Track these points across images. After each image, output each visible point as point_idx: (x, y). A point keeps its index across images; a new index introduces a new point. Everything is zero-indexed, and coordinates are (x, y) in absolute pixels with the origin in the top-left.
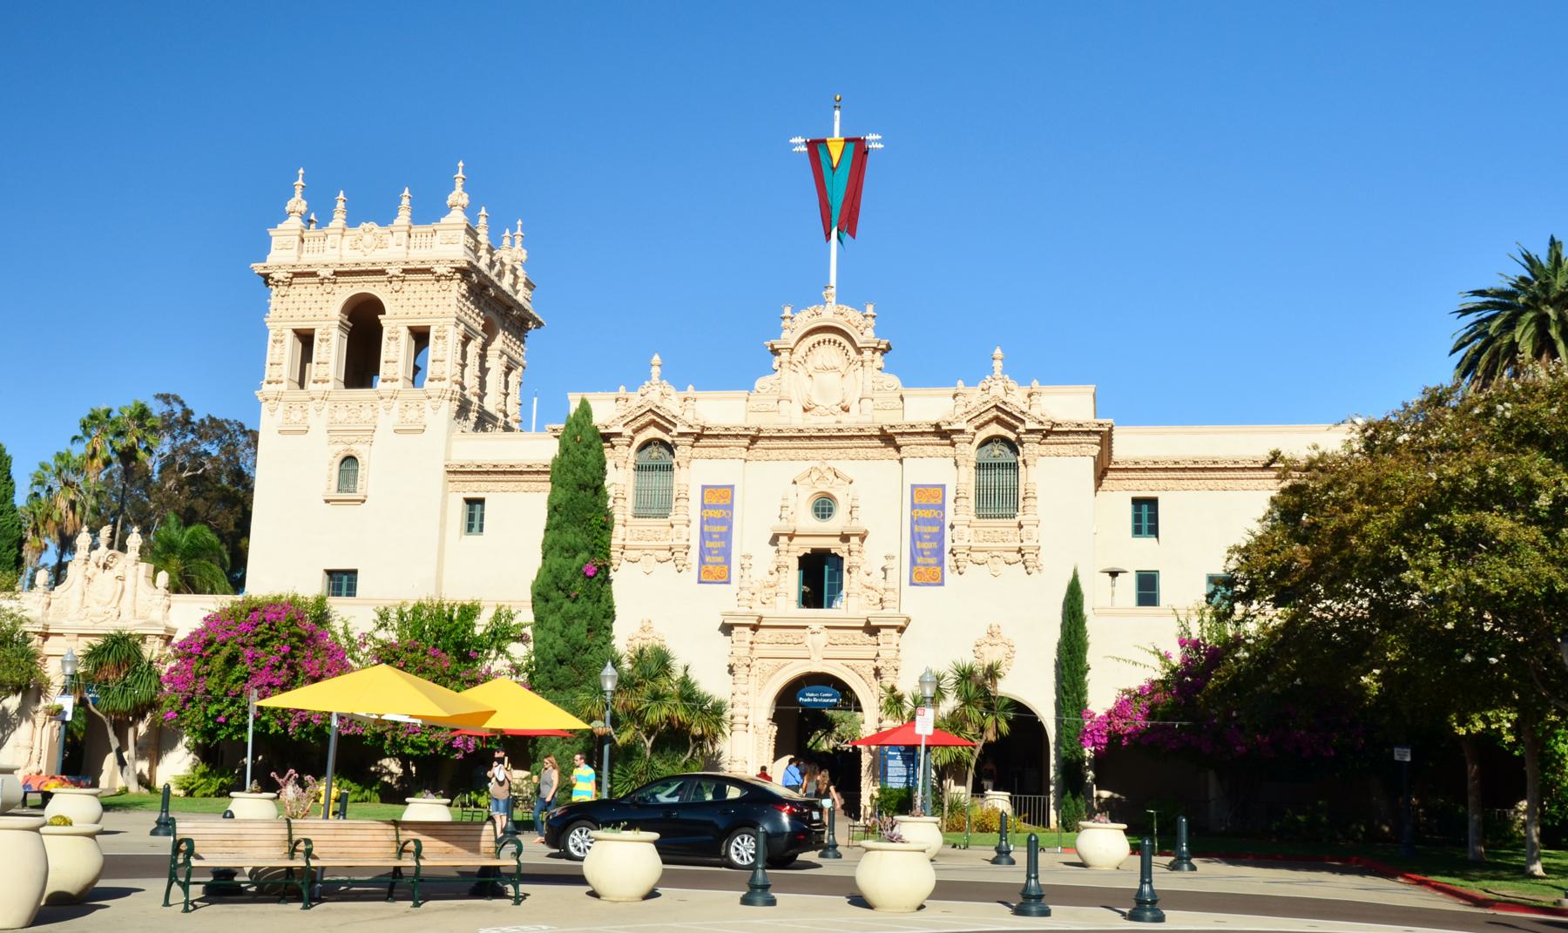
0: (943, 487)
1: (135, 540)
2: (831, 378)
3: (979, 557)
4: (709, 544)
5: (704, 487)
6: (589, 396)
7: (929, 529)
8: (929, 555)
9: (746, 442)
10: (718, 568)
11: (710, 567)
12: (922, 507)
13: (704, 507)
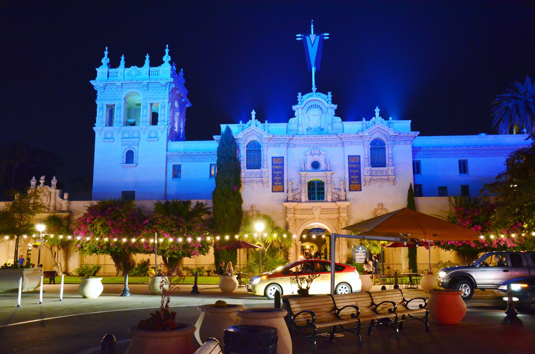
0: (359, 156)
1: (54, 182)
4: (275, 178)
5: (272, 158)
6: (231, 126)
7: (355, 171)
8: (355, 181)
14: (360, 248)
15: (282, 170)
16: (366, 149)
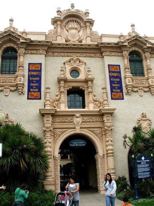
2: (74, 31)
3: (136, 89)
4: (32, 84)
5: (29, 64)
7: (116, 80)
8: (117, 89)
9: (46, 48)
10: (36, 94)
11: (33, 93)
12: (113, 72)
13: (29, 71)
14: (143, 158)
15: (40, 77)
16: (126, 60)
